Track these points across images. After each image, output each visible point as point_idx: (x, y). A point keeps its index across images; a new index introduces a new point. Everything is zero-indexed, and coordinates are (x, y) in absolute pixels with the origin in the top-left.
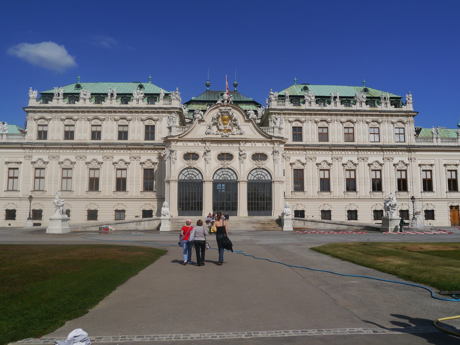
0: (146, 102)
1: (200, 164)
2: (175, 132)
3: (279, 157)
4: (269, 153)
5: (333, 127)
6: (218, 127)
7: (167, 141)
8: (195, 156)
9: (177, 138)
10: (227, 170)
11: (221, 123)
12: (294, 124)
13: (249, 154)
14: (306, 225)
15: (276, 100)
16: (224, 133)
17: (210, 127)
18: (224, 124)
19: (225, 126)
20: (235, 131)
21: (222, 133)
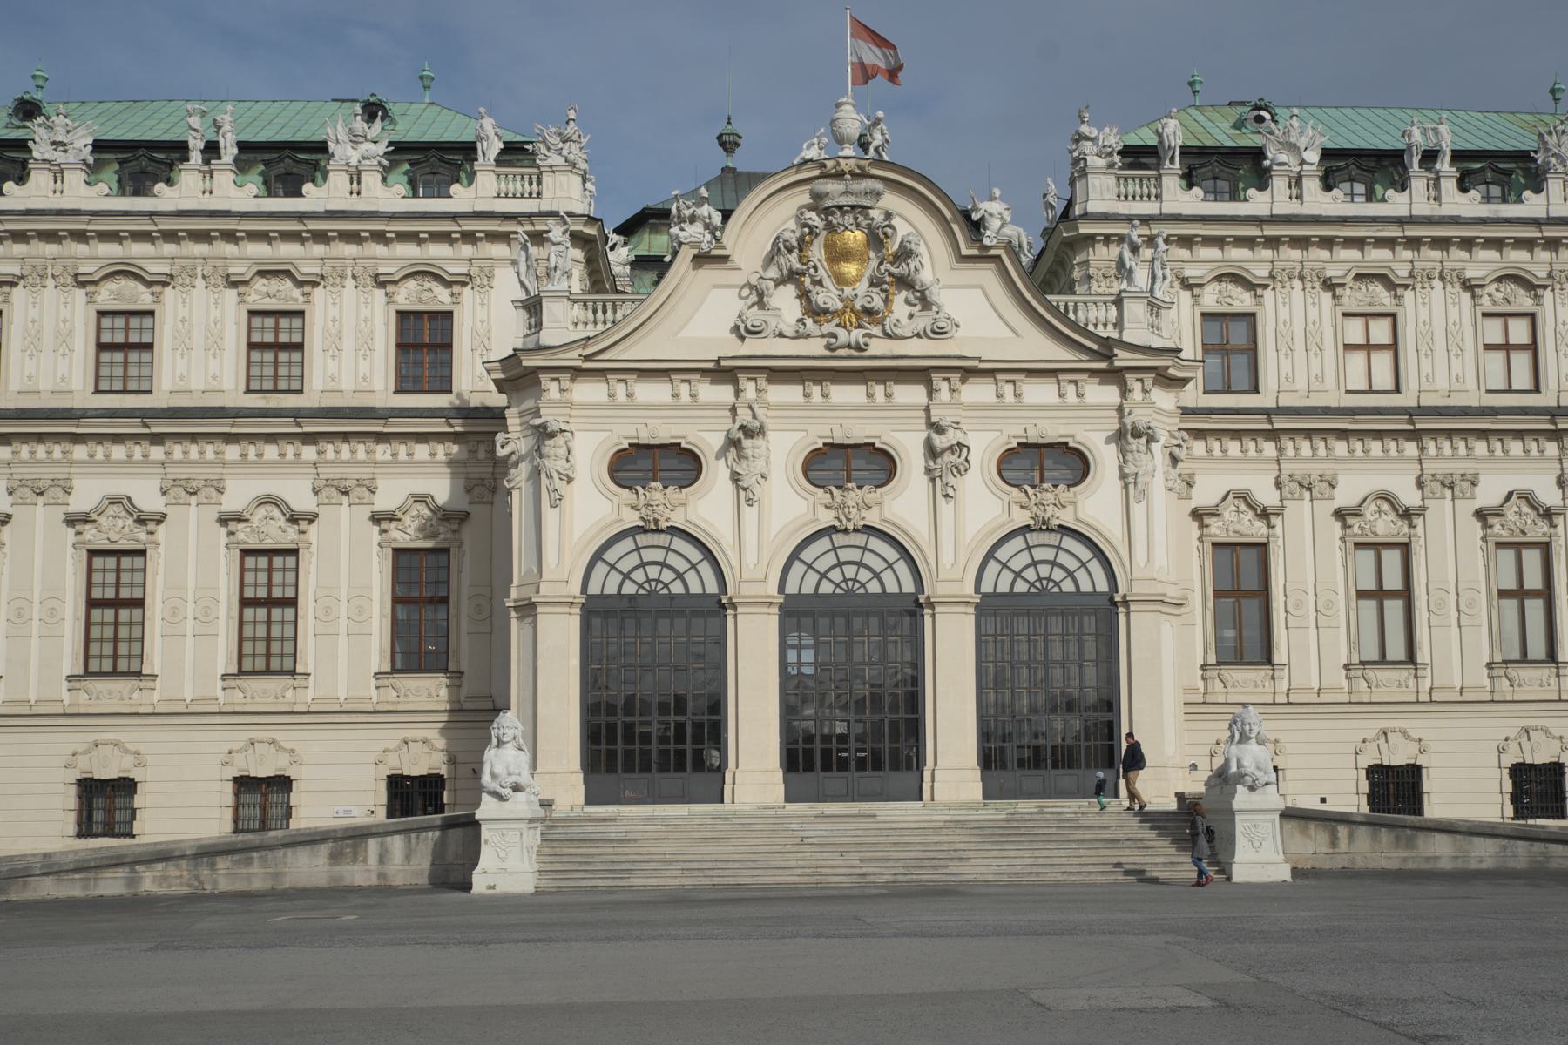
0: (402, 188)
1: (707, 507)
2: (564, 323)
3: (1153, 463)
4: (1096, 441)
5: (1423, 314)
6: (804, 295)
7: (518, 376)
8: (679, 464)
9: (572, 358)
10: (860, 539)
11: (822, 273)
12: (1211, 299)
13: (985, 445)
14: (1343, 845)
15: (1111, 166)
16: (841, 333)
17: (761, 295)
18: (841, 280)
19: (848, 291)
20: (904, 321)
21: (828, 328)
